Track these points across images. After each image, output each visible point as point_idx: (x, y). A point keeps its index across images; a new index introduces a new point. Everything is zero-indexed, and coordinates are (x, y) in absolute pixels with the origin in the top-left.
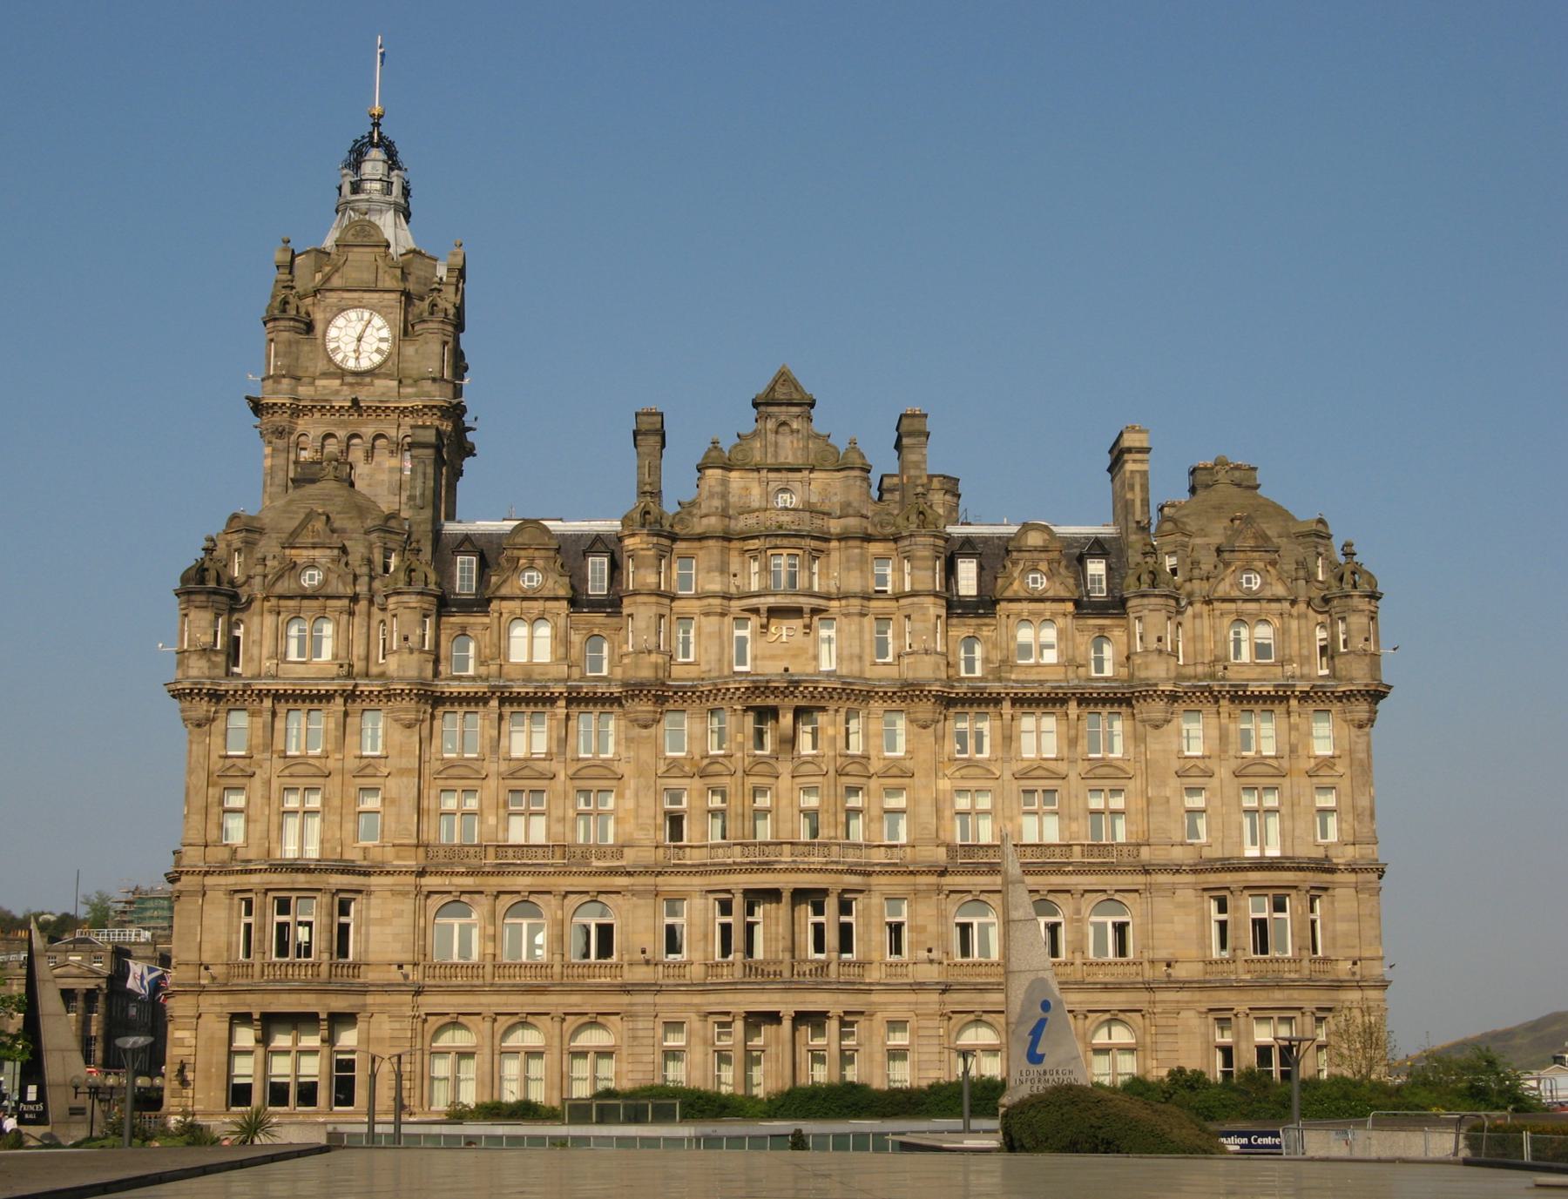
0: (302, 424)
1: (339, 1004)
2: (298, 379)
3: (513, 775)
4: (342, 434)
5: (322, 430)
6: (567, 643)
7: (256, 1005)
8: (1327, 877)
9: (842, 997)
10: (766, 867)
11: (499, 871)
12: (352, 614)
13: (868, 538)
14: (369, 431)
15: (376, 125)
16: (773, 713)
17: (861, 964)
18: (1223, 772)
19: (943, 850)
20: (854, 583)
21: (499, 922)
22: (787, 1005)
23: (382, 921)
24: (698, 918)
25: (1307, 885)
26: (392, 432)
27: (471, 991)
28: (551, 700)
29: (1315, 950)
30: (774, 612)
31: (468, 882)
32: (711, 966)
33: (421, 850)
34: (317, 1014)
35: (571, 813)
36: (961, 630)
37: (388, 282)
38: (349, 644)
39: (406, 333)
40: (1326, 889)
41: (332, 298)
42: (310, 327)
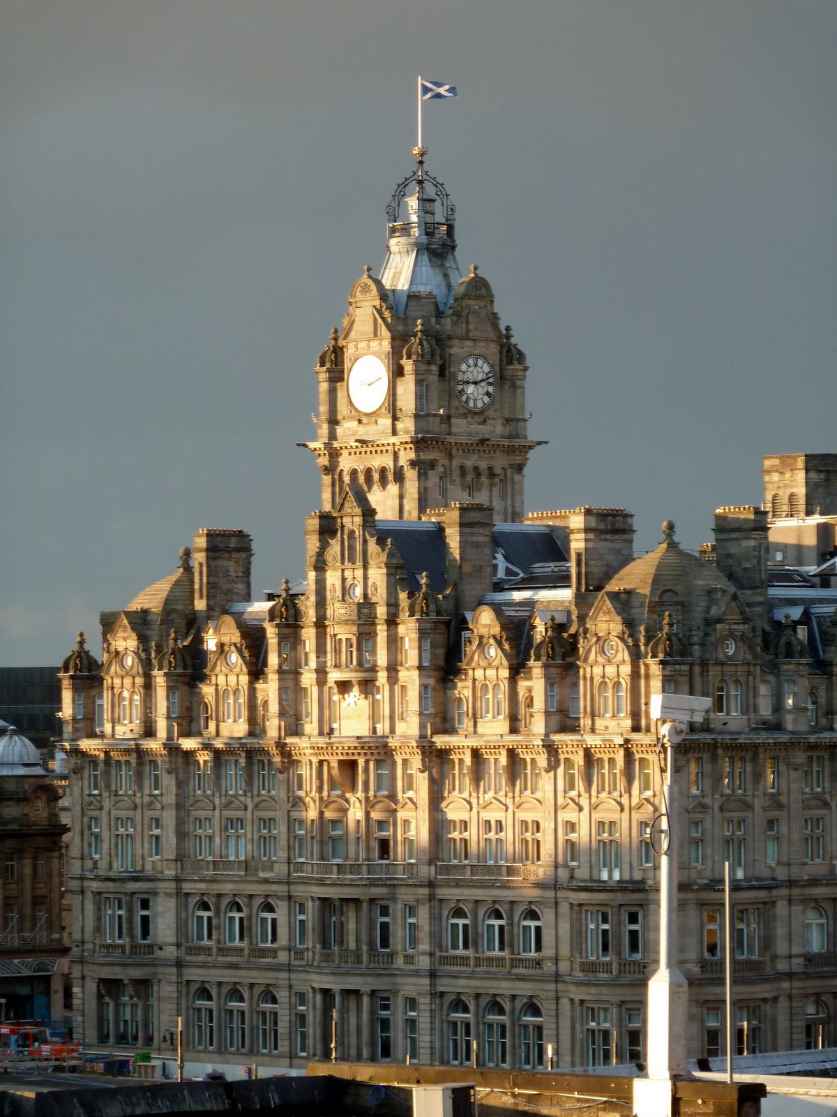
1: (137, 973)
3: (227, 806)
8: (640, 896)
9: (369, 979)
11: (213, 880)
15: (421, 162)
19: (433, 868)
21: (222, 915)
25: (616, 903)
27: (204, 965)
30: (344, 686)
33: (179, 863)
34: (122, 980)
35: (256, 837)
39: (397, 372)
40: (641, 905)
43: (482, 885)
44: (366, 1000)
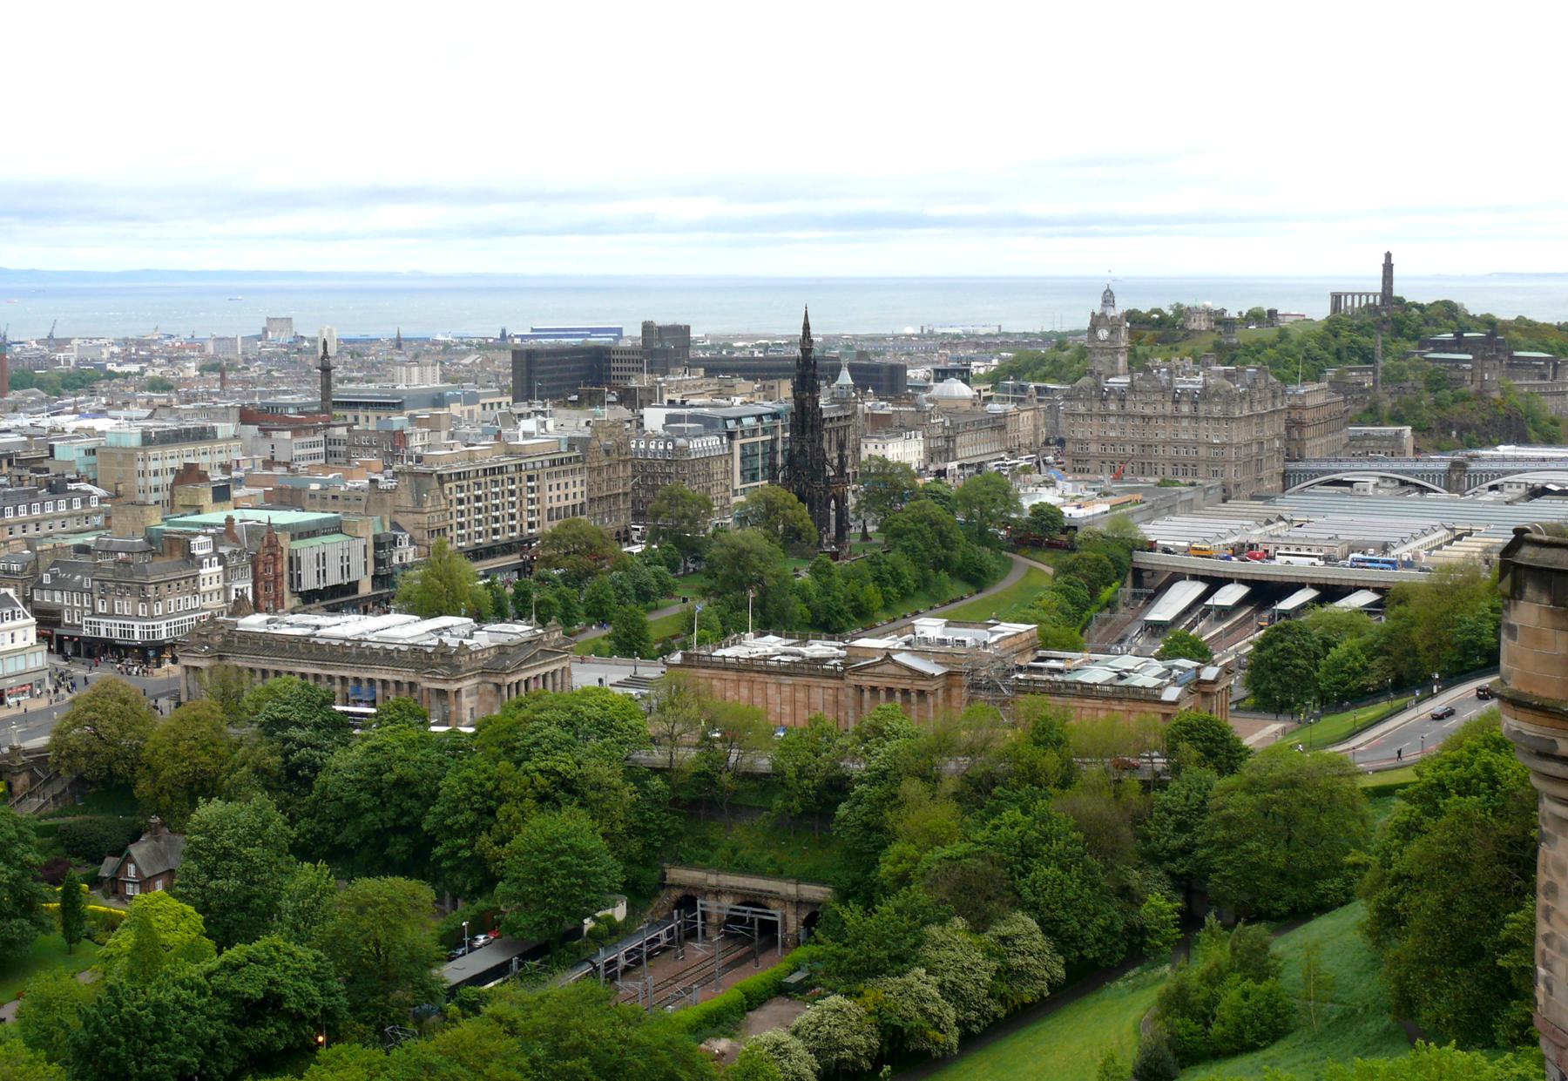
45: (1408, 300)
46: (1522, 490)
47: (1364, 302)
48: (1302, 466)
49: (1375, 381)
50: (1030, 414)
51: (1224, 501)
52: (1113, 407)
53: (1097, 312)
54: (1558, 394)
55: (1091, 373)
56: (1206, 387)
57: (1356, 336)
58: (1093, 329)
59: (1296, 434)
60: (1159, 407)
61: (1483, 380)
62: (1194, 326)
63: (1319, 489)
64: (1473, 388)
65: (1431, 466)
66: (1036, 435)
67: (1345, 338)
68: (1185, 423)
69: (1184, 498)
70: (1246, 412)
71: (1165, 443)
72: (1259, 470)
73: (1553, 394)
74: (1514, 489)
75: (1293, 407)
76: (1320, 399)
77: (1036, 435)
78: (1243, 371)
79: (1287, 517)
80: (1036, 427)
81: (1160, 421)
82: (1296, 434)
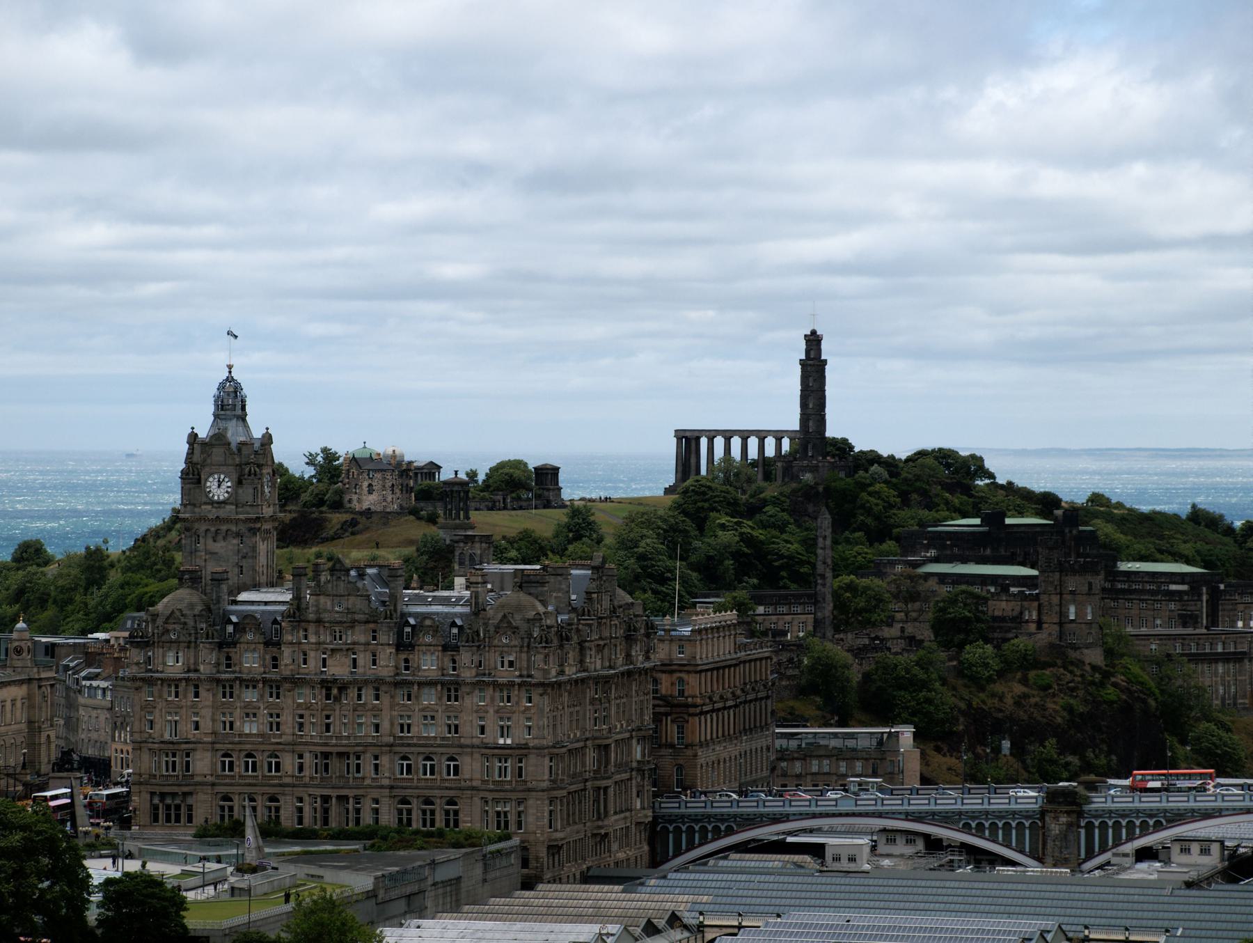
0: (196, 525)
1: (186, 789)
2: (194, 505)
4: (213, 529)
5: (203, 528)
6: (264, 659)
7: (157, 789)
10: (326, 745)
11: (240, 743)
12: (188, 647)
13: (367, 622)
14: (224, 528)
16: (329, 689)
17: (363, 778)
18: (491, 711)
20: (362, 639)
22: (334, 793)
23: (202, 760)
24: (308, 759)
26: (234, 529)
27: (231, 785)
28: (258, 681)
29: (520, 776)
31: (230, 746)
32: (312, 778)
36: (403, 656)
37: (230, 462)
38: (189, 659)
39: (240, 482)
41: (207, 469)
42: (199, 481)
43: (420, 746)
44: (351, 800)
45: (860, 445)
46: (1213, 860)
47: (770, 451)
48: (693, 805)
49: (817, 623)
50: (18, 692)
51: (528, 884)
52: (251, 662)
53: (203, 433)
54: (1226, 658)
55: (192, 579)
56: (478, 609)
57: (748, 526)
58: (193, 476)
59: (671, 731)
60: (363, 659)
61: (1062, 622)
62: (369, 501)
63: (736, 860)
64: (1044, 637)
65: (999, 803)
66: (33, 745)
67: (725, 533)
68: (429, 698)
69: (443, 874)
70: (571, 671)
71: (380, 747)
72: (601, 815)
73: (1214, 659)
74: (1195, 857)
75: (668, 667)
76: (722, 650)
77: (33, 745)
78: (562, 573)
79: (690, 918)
80: (33, 727)
81: (368, 695)
82: (671, 731)
